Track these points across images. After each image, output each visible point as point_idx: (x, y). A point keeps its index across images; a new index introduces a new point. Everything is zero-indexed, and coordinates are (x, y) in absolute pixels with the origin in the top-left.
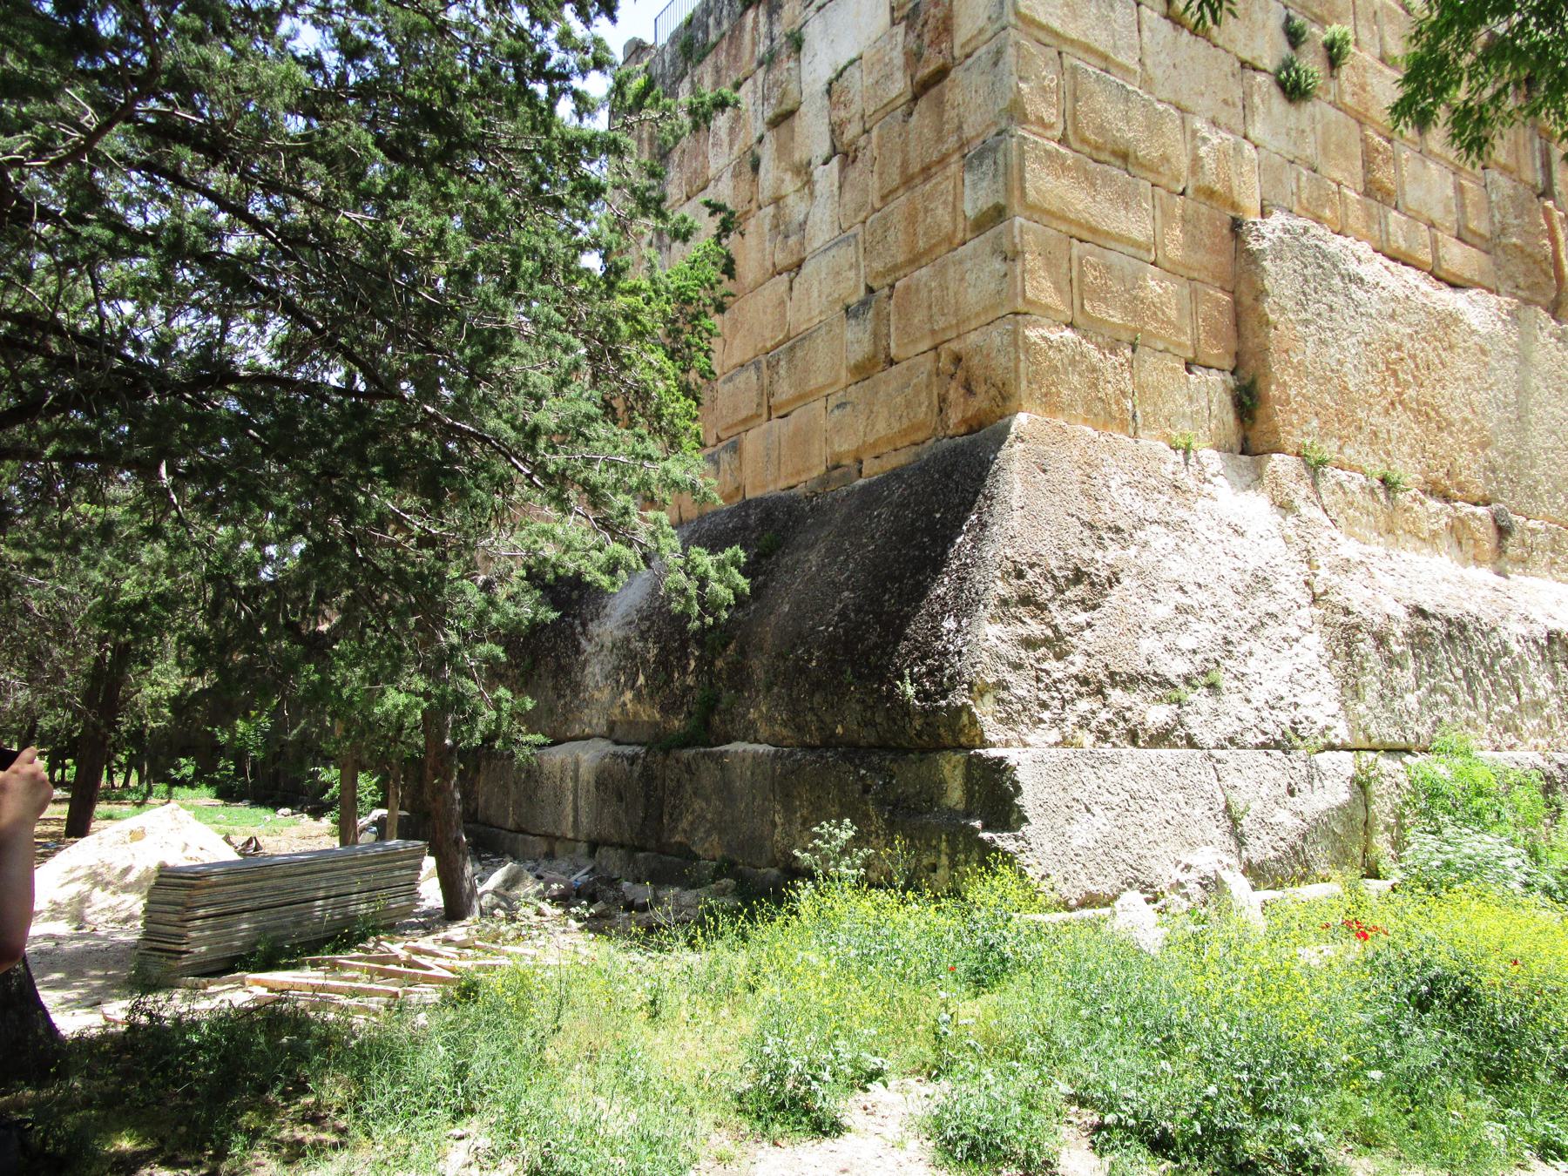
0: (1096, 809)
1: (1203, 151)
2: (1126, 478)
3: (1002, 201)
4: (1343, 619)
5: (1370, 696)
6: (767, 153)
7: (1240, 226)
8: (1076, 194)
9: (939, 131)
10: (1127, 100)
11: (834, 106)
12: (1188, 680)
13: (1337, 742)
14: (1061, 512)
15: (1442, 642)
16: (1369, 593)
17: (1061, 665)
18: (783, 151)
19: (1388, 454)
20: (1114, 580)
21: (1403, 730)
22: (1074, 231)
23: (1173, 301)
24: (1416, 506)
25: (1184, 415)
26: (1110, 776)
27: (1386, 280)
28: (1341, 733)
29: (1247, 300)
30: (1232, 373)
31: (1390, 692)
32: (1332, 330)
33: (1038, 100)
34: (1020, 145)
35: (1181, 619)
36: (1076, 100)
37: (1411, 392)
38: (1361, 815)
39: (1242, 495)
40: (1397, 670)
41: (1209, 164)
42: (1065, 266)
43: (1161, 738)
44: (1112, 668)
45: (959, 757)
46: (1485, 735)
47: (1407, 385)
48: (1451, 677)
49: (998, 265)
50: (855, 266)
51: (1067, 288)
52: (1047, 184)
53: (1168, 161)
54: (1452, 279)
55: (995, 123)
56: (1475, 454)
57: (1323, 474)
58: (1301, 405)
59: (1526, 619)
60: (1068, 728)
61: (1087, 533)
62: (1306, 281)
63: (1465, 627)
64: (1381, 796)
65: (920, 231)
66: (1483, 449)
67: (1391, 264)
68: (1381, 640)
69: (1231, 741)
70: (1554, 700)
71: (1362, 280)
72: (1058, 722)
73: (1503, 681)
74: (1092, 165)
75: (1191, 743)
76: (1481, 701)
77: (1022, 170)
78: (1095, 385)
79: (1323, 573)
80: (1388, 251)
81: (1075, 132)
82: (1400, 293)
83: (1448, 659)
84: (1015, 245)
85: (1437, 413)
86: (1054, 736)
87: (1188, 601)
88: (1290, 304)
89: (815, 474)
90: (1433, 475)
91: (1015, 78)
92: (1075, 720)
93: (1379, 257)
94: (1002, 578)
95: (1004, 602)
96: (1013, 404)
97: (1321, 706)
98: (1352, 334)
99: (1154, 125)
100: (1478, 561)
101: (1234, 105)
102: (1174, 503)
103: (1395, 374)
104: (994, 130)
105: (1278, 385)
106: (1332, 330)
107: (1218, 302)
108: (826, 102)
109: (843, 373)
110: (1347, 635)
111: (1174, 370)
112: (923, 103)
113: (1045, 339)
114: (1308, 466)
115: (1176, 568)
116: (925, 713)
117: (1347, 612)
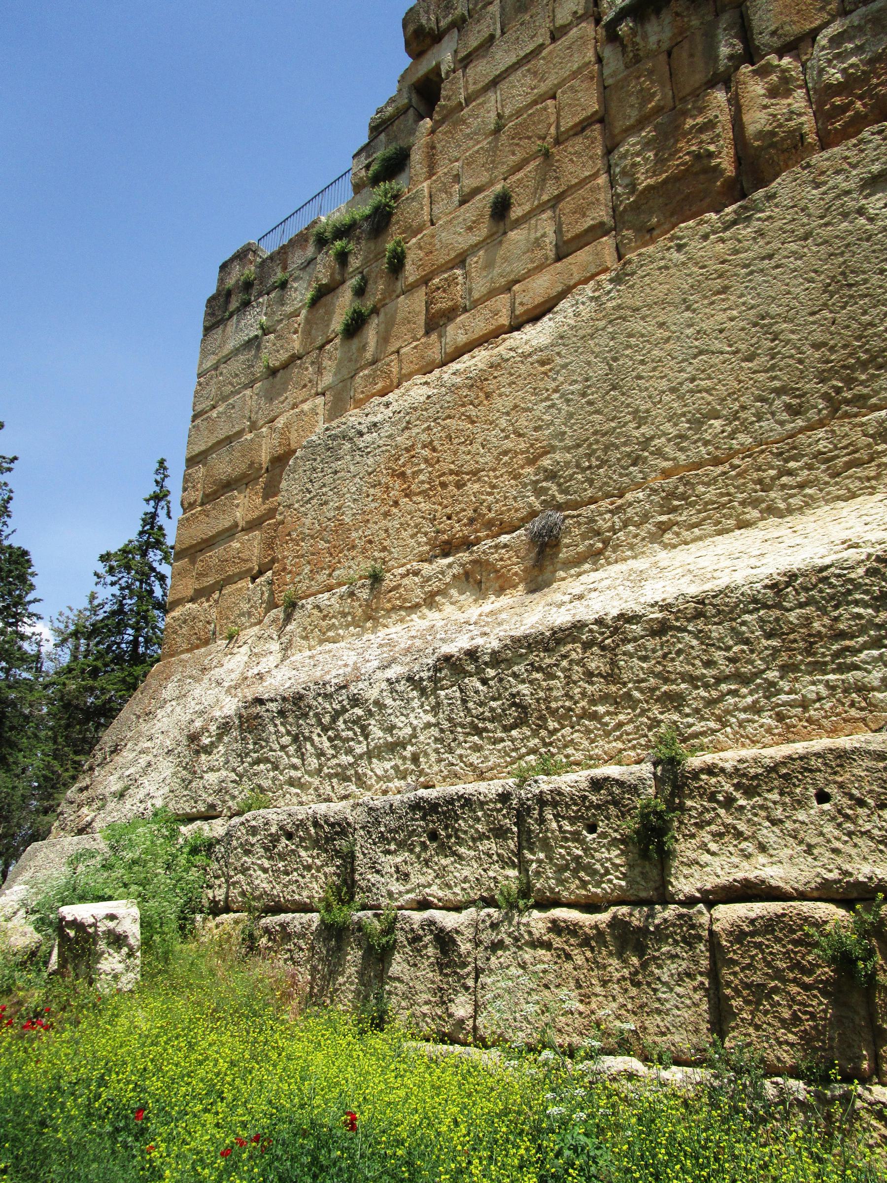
54: (532, 315)
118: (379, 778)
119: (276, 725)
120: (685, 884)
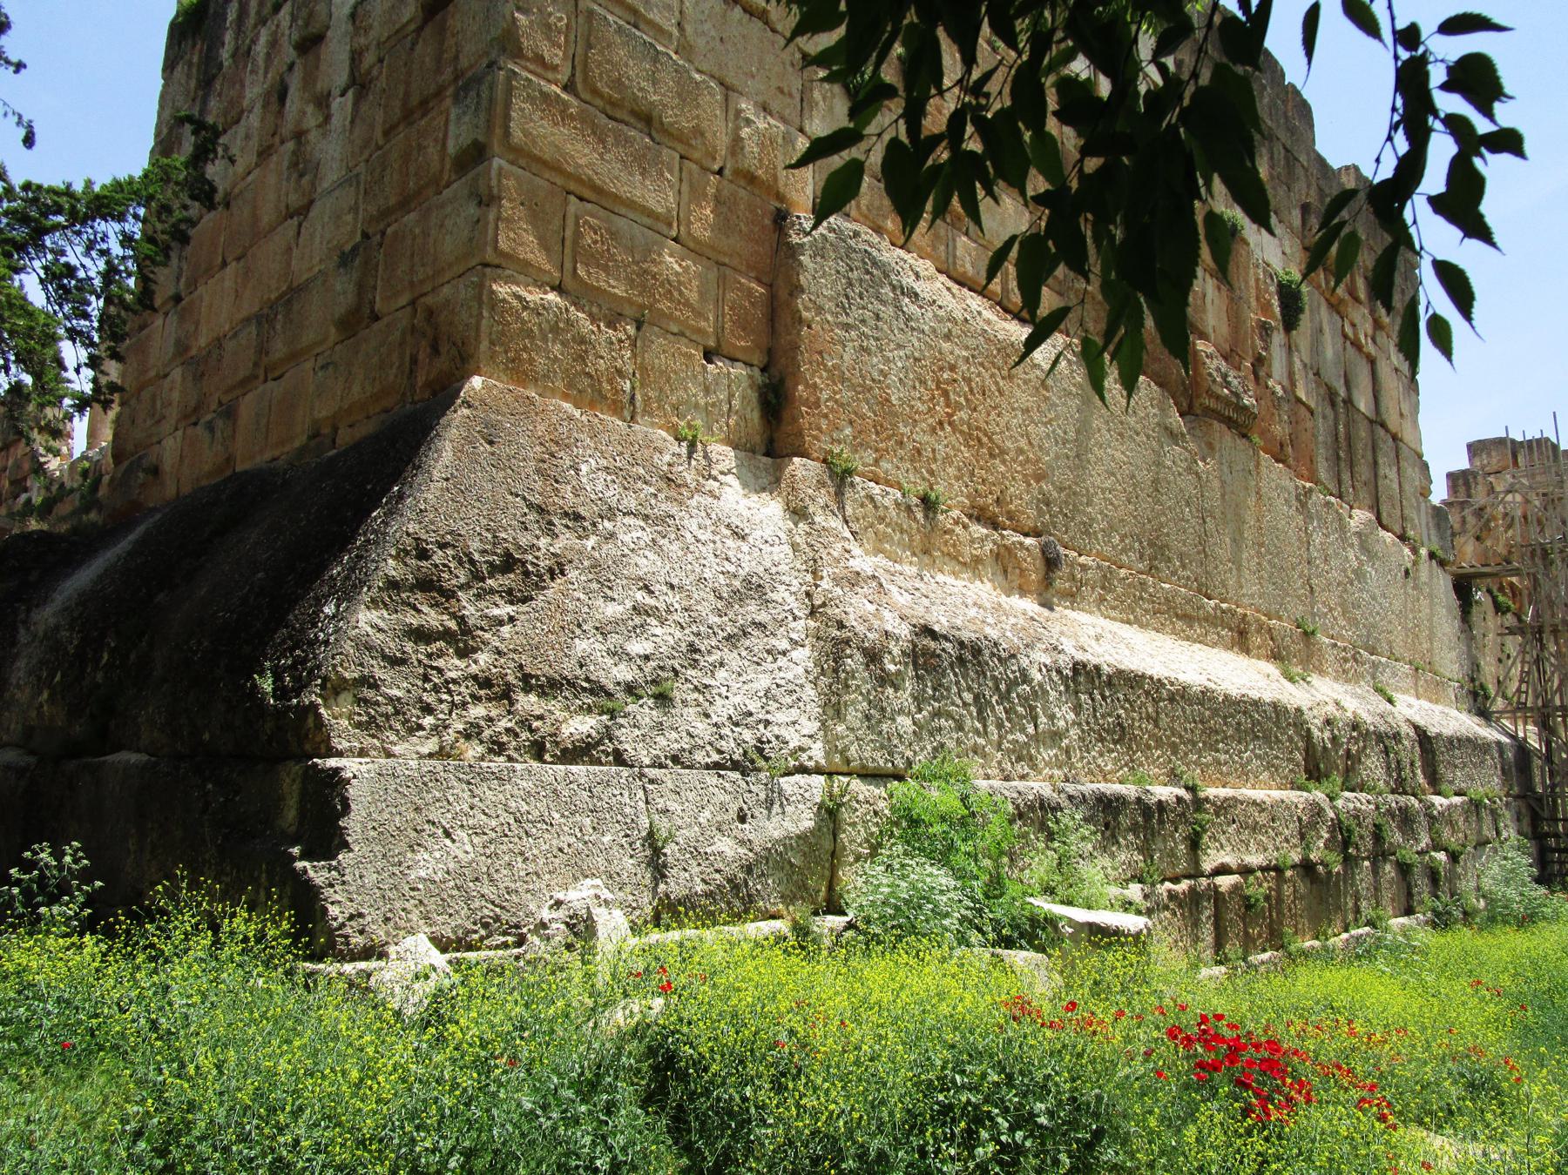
0: (460, 834)
1: (745, 132)
2: (604, 463)
3: (481, 138)
4: (835, 633)
5: (853, 716)
6: (295, 83)
7: (784, 218)
8: (579, 146)
9: (438, 60)
10: (655, 60)
11: (357, 30)
12: (630, 689)
13: (811, 764)
14: (503, 490)
15: (952, 665)
16: (871, 608)
17: (461, 664)
18: (309, 80)
19: (932, 473)
20: (558, 569)
21: (891, 754)
22: (572, 186)
23: (695, 283)
24: (958, 529)
25: (697, 406)
26: (488, 793)
27: (946, 300)
28: (817, 752)
29: (783, 294)
30: (763, 370)
31: (877, 714)
32: (877, 339)
33: (539, 36)
34: (508, 80)
35: (638, 620)
36: (590, 46)
37: (963, 414)
38: (827, 844)
39: (755, 497)
40: (890, 691)
41: (752, 147)
42: (557, 222)
43: (580, 752)
44: (528, 670)
45: (296, 768)
46: (994, 763)
47: (959, 407)
48: (959, 702)
49: (472, 210)
50: (354, 209)
51: (558, 248)
52: (532, 125)
53: (702, 134)
55: (487, 53)
56: (1029, 485)
57: (852, 485)
58: (832, 410)
59: (1055, 648)
60: (449, 736)
61: (532, 516)
62: (850, 284)
63: (979, 651)
64: (854, 824)
65: (412, 169)
66: (1038, 482)
67: (955, 288)
68: (873, 656)
69: (675, 759)
70: (1074, 733)
71: (916, 295)
72: (436, 730)
73: (1019, 709)
74: (603, 120)
75: (619, 759)
76: (992, 728)
77: (508, 106)
78: (581, 358)
79: (826, 584)
80: (955, 275)
81: (585, 79)
82: (958, 315)
83: (957, 683)
84: (490, 188)
85: (990, 439)
86: (431, 745)
87: (653, 602)
88: (829, 305)
89: (297, 444)
90: (980, 501)
91: (510, 6)
92: (461, 727)
93: (943, 278)
94: (395, 558)
95: (393, 585)
96: (472, 366)
97: (797, 727)
98: (900, 346)
99: (687, 93)
100: (1023, 592)
101: (791, 95)
102: (661, 496)
103: (945, 394)
104: (485, 62)
105: (807, 386)
106: (877, 339)
107: (750, 291)
108: (351, 28)
109: (333, 330)
110: (837, 649)
111: (690, 356)
112: (428, 30)
113: (519, 298)
114: (833, 474)
115: (646, 563)
116: (280, 714)
117: (841, 625)
118: (1047, 764)
119: (956, 675)
120: (1207, 866)
